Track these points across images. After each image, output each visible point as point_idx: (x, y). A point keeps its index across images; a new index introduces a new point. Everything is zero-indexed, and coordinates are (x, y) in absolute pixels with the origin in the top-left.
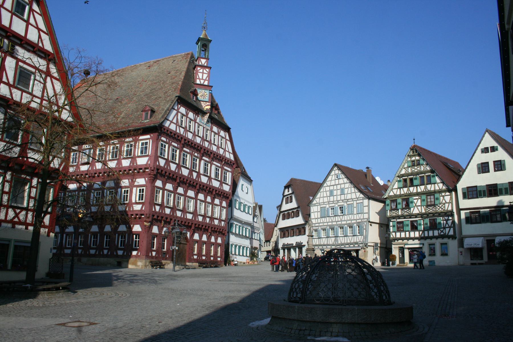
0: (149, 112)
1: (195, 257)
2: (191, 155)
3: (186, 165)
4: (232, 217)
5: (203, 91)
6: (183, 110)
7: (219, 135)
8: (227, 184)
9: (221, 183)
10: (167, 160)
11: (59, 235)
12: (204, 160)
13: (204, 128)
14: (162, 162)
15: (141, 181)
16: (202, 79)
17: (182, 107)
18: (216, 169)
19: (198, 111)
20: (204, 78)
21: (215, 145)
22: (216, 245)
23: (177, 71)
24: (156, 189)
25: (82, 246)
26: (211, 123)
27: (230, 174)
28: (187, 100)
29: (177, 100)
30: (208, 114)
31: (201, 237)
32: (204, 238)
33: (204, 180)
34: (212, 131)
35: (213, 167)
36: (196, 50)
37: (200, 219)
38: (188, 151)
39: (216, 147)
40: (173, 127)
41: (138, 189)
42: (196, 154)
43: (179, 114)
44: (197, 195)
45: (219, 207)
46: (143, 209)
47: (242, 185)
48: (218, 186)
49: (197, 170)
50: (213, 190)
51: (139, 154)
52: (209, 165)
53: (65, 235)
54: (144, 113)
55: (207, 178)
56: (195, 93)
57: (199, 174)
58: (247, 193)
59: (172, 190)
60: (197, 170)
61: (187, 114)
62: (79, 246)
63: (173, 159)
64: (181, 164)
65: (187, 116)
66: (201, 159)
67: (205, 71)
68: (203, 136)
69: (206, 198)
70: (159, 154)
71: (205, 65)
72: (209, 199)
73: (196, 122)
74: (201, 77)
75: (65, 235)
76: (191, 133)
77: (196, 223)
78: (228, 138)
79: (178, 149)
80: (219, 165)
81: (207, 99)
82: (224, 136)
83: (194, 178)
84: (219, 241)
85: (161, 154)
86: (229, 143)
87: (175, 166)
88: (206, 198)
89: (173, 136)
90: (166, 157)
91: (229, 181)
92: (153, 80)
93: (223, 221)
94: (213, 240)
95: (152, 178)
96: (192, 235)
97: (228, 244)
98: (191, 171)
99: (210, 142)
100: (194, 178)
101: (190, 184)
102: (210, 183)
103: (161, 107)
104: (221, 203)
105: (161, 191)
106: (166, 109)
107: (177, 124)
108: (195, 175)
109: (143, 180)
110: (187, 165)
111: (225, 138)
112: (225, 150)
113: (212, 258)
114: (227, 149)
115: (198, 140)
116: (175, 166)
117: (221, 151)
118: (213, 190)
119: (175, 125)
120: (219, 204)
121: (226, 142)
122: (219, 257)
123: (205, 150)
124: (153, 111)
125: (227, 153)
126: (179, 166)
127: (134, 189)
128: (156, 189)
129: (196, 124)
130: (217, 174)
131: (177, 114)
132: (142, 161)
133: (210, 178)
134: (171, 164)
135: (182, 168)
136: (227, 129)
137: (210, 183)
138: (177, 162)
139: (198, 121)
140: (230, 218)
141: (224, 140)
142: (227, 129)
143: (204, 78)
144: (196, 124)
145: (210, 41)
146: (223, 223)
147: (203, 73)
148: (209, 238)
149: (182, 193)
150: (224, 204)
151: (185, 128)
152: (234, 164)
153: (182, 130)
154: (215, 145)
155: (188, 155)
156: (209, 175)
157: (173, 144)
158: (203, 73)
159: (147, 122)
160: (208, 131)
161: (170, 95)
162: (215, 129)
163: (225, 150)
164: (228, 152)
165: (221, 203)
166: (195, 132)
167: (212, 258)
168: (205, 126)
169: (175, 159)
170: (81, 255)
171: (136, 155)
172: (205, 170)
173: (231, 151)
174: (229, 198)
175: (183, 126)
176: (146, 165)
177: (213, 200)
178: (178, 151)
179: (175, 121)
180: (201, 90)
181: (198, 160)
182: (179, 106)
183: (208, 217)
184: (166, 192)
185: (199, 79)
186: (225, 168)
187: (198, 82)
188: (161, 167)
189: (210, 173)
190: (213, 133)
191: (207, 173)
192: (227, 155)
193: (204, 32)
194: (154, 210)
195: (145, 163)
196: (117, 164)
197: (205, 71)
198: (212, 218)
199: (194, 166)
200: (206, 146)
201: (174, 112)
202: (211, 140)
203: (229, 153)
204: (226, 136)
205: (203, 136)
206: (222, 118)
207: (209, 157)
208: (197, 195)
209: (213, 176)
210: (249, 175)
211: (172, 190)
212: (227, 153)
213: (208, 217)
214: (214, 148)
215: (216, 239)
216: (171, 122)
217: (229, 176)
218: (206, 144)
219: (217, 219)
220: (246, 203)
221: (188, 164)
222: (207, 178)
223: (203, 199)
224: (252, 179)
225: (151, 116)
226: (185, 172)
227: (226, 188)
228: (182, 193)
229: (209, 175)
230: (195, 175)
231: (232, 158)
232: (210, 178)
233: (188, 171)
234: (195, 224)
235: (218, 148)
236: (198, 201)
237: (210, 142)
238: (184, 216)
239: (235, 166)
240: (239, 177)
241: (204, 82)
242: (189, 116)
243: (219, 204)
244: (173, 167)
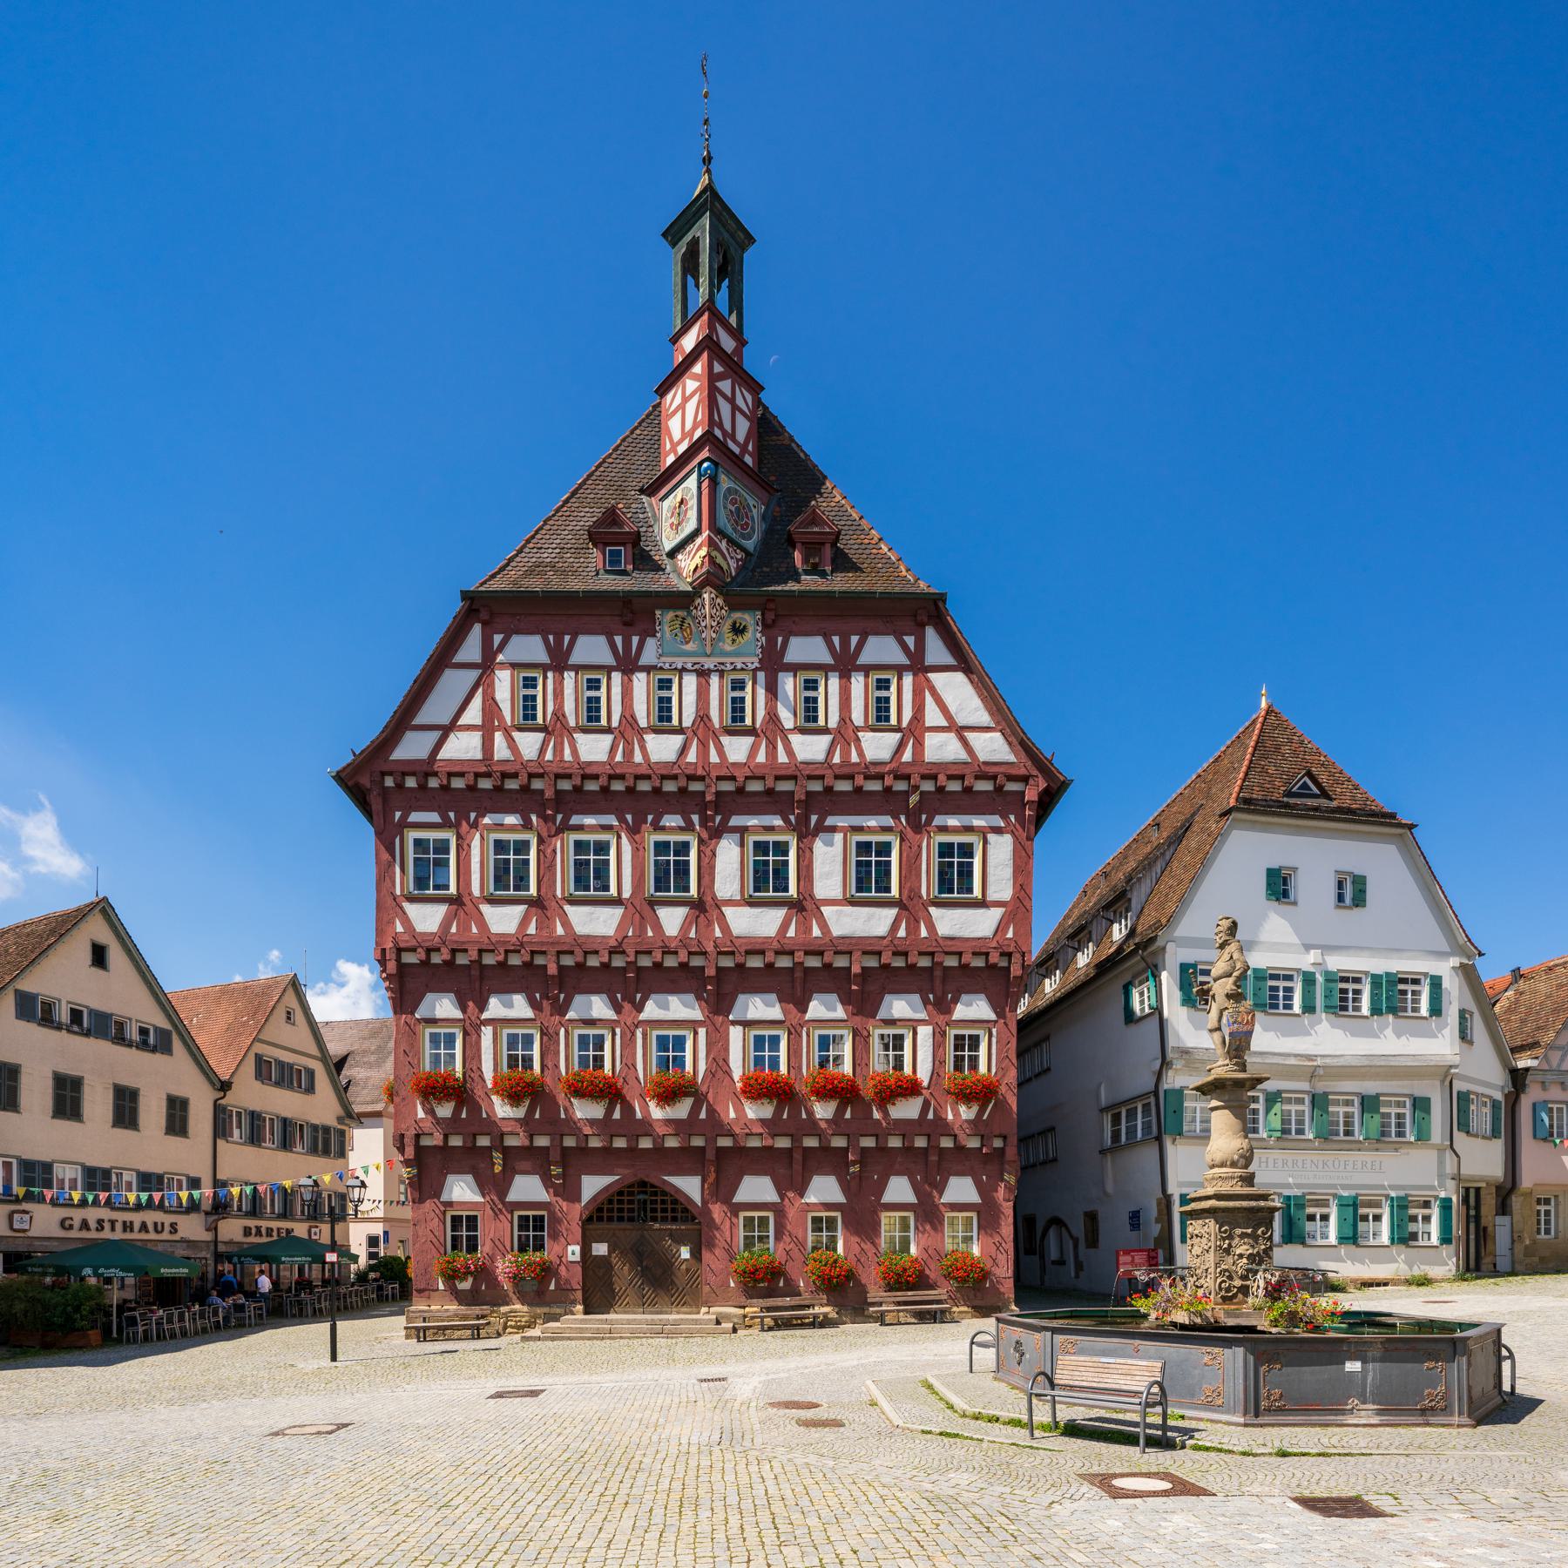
8: (983, 904)
14: (427, 918)
78: (935, 650)
114: (933, 716)
139: (649, 656)
168: (709, 663)
192: (941, 748)
203: (960, 731)
205: (703, 717)
218: (737, 749)
226: (596, 923)
230: (672, 920)
231: (993, 747)
232: (804, 906)
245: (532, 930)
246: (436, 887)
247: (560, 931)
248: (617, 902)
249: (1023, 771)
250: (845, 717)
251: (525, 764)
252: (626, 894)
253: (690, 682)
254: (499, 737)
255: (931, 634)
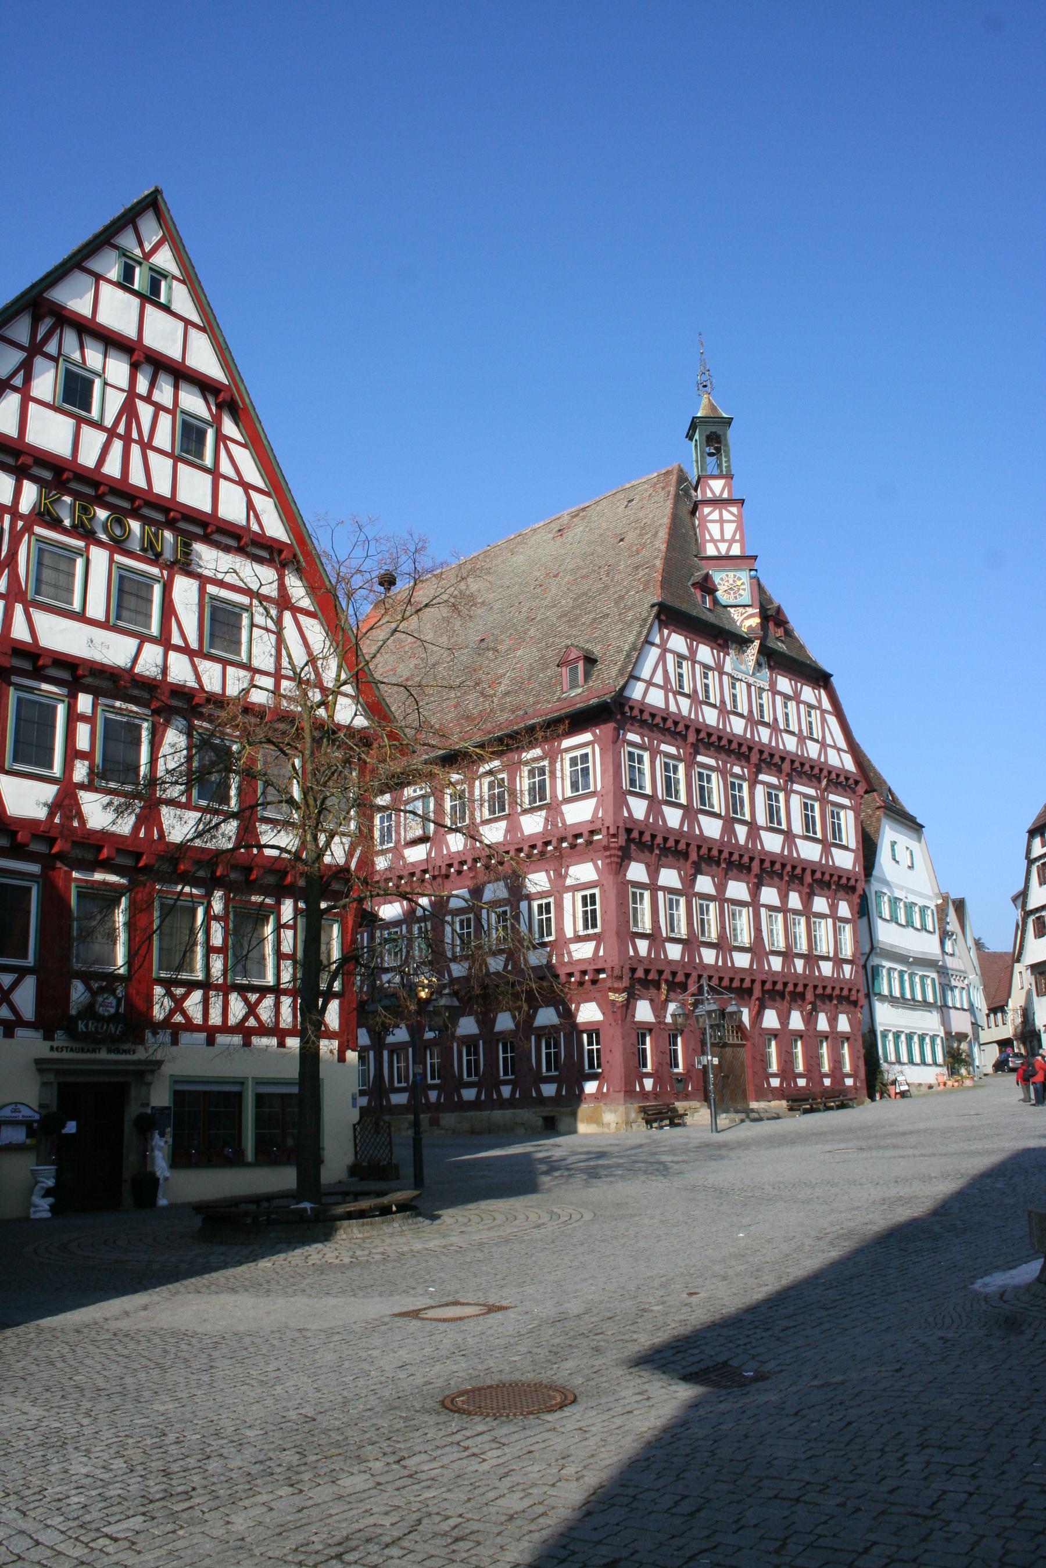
0: (581, 665)
1: (775, 1082)
2: (723, 773)
3: (712, 806)
4: (872, 948)
5: (731, 574)
6: (678, 642)
7: (799, 702)
8: (846, 848)
9: (827, 847)
10: (652, 799)
11: (371, 1053)
12: (763, 783)
13: (749, 686)
14: (638, 808)
15: (583, 872)
16: (723, 540)
17: (674, 636)
18: (806, 804)
19: (723, 637)
20: (728, 536)
21: (792, 733)
22: (835, 1038)
23: (643, 528)
24: (631, 890)
25: (437, 1081)
26: (771, 668)
27: (851, 814)
28: (687, 611)
29: (657, 617)
30: (757, 643)
31: (784, 1018)
32: (796, 1021)
33: (772, 843)
34: (775, 692)
35: (795, 801)
36: (689, 456)
37: (776, 964)
38: (712, 762)
39: (795, 739)
40: (656, 698)
41: (579, 895)
42: (737, 770)
43: (670, 657)
44: (755, 893)
45: (830, 921)
46: (601, 953)
47: (893, 844)
48: (816, 858)
49: (748, 818)
50: (804, 870)
51: (569, 793)
52: (782, 796)
53: (385, 1053)
54: (565, 671)
55: (780, 838)
56: (707, 587)
57: (753, 828)
58: (911, 867)
59: (678, 885)
60: (748, 818)
61: (693, 652)
62: (429, 1081)
63: (669, 794)
64: (696, 804)
65: (692, 658)
66: (753, 783)
67: (726, 516)
68: (751, 711)
69: (784, 897)
70: (625, 785)
71: (725, 495)
72: (795, 900)
73: (721, 673)
74: (717, 536)
75: (385, 1053)
76: (714, 706)
77: (764, 977)
78: (826, 705)
79: (681, 760)
80: (811, 792)
81: (745, 597)
82: (815, 703)
83: (742, 841)
84: (843, 1024)
85: (632, 783)
86: (832, 720)
87: (679, 812)
88: (784, 897)
89: (661, 725)
90: (648, 791)
91: (850, 836)
92: (579, 568)
93: (847, 961)
94: (822, 1024)
95: (615, 859)
96: (757, 1017)
97: (873, 1031)
98: (729, 824)
99: (773, 727)
100: (742, 841)
101: (730, 863)
102: (790, 851)
103: (612, 643)
104: (833, 907)
105: (647, 894)
106: (627, 648)
107: (666, 687)
108: (741, 831)
109: (589, 866)
110: (714, 805)
111: (819, 707)
112: (823, 745)
113: (827, 1082)
114: (829, 741)
115: (738, 726)
116: (679, 812)
117: (813, 750)
118: (804, 870)
119: (662, 692)
120: (827, 911)
121: (824, 720)
122: (849, 1076)
123: (761, 752)
124: (590, 661)
125: (832, 753)
126: (690, 813)
127: (567, 897)
128: (631, 890)
129: (725, 678)
130: (808, 822)
131: (662, 658)
132: (579, 813)
133: (789, 836)
134: (666, 809)
135: (701, 817)
136: (821, 679)
137: (790, 851)
138: (683, 800)
139: (728, 668)
140: (867, 950)
141: (816, 715)
142: (821, 679)
143: (728, 536)
144: (725, 678)
145: (729, 422)
146: (847, 968)
147: (722, 521)
148: (810, 1019)
149: (712, 891)
150: (844, 909)
151: (692, 696)
152: (857, 783)
153: (685, 703)
154: (792, 733)
155: (714, 776)
156: (784, 827)
157: (664, 747)
158: (722, 521)
159: (579, 694)
160: (764, 695)
161: (634, 605)
162: (784, 684)
163: (823, 745)
164: (835, 747)
165: (833, 907)
166: (723, 702)
167: (827, 1082)
168: (751, 680)
169: (677, 791)
170: (437, 1107)
171: (560, 798)
172: (772, 813)
173: (842, 743)
174: (855, 890)
175: (686, 690)
176: (592, 822)
177: (807, 901)
178: (681, 767)
179: (659, 679)
180: (723, 575)
181: (745, 785)
182: (666, 632)
183: (800, 956)
184: (660, 894)
185: (713, 540)
186: (832, 797)
187: (711, 550)
188: (635, 821)
189: (788, 822)
190: (778, 698)
191: (779, 823)
193: (705, 401)
194: (632, 953)
195: (588, 817)
196: (507, 831)
197: (726, 516)
198: (812, 959)
199: (734, 805)
200: (765, 740)
201: (654, 653)
202: (776, 719)
203: (839, 750)
204: (819, 701)
205: (751, 711)
206: (802, 647)
207: (778, 770)
208: (755, 893)
209: (798, 828)
210: (911, 810)
211: (678, 885)
212: (832, 753)
213: (800, 956)
214: (790, 744)
215: (833, 1021)
216: (650, 683)
217: (848, 821)
218: (764, 735)
219: (826, 958)
220: (912, 899)
221: (718, 802)
222: (780, 838)
223: (776, 902)
224: (919, 821)
225: (587, 675)
226: (711, 828)
227: (845, 860)
228: (712, 891)
229: (784, 827)
230: (741, 831)
231: (849, 765)
232: (789, 836)
233: (719, 823)
234: (764, 983)
235: (801, 739)
236: (763, 910)
237: (773, 727)
238: (725, 961)
239: (861, 789)
240: (879, 820)
241: (729, 549)
242: (803, 698)
243: (827, 911)
244: (673, 817)
245: (685, 829)
246: (641, 788)
247: (697, 832)
248: (717, 816)
249: (858, 778)
250: (800, 730)
251: (683, 717)
252: (723, 814)
253: (744, 685)
254: (670, 694)
255: (822, 691)
